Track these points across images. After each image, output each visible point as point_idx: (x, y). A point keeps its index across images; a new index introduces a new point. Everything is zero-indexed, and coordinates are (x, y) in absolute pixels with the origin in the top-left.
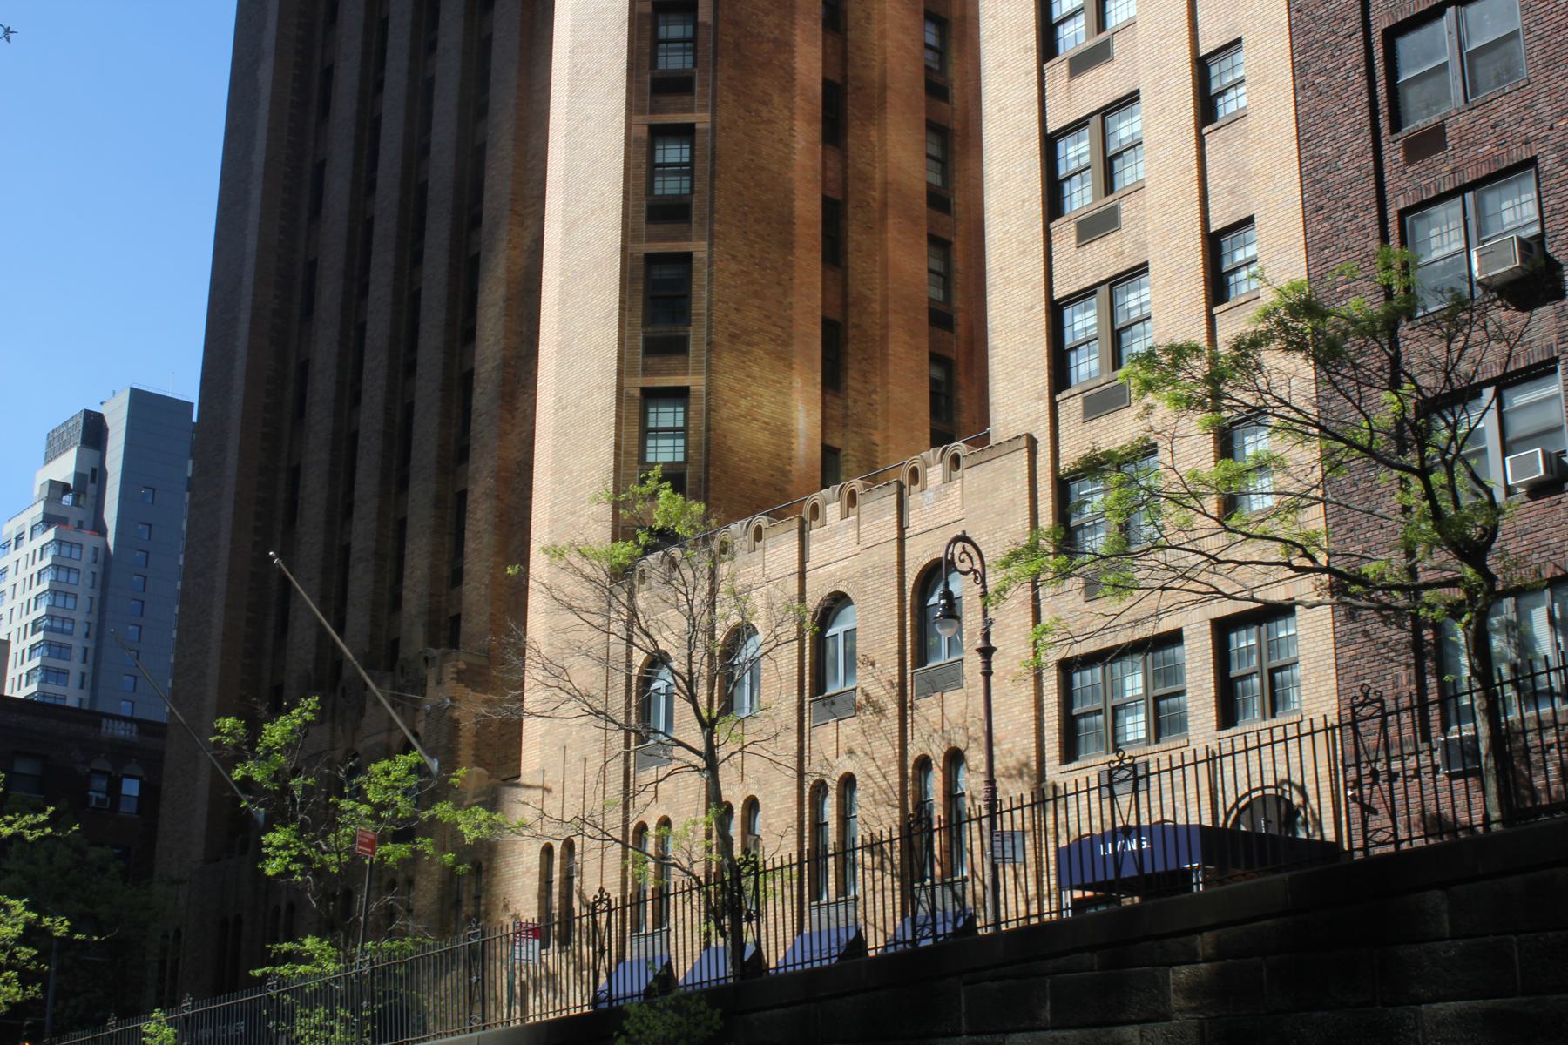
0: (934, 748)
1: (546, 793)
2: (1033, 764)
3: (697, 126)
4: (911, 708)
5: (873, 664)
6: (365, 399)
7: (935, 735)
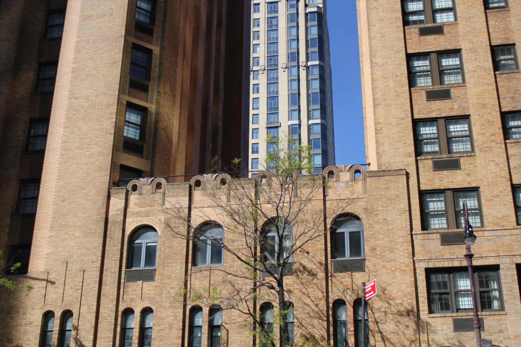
1: (49, 284)
2: (415, 310)
4: (331, 276)
7: (348, 291)
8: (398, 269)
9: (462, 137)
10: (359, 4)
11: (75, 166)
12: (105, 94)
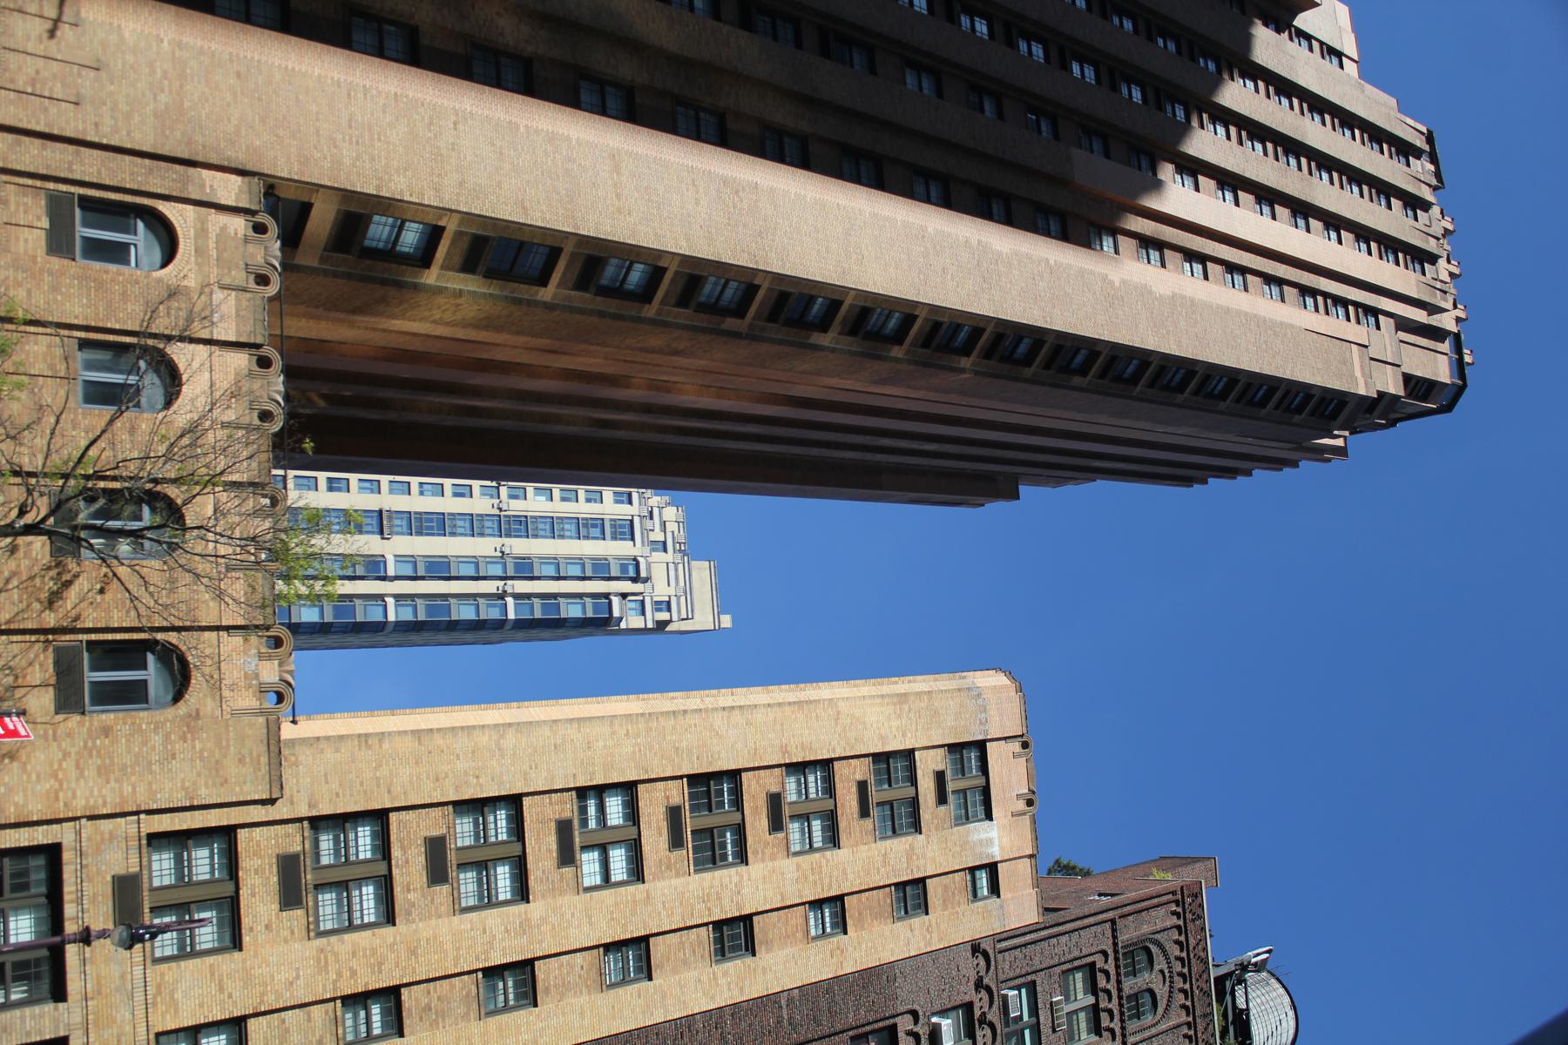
1: (49, 25)
3: (647, 306)
8: (61, 785)
9: (810, 837)
10: (989, 676)
11: (314, 108)
12: (462, 183)
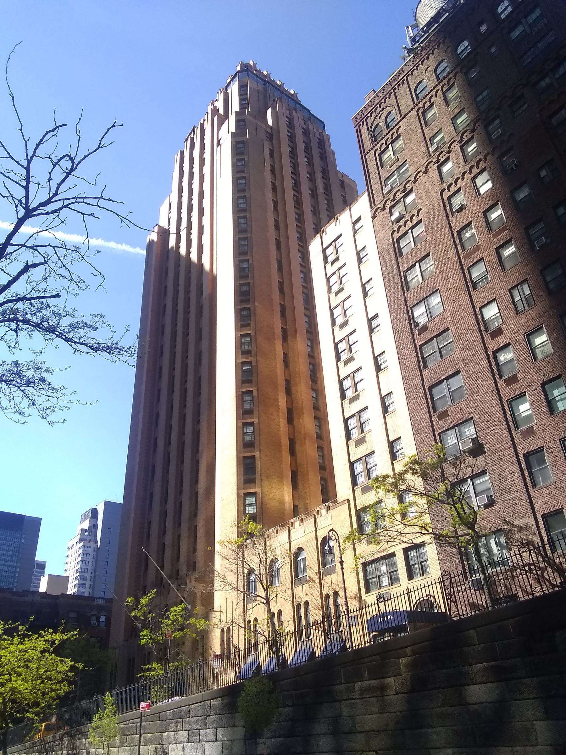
0: (330, 591)
5: (311, 568)
6: (168, 502)
